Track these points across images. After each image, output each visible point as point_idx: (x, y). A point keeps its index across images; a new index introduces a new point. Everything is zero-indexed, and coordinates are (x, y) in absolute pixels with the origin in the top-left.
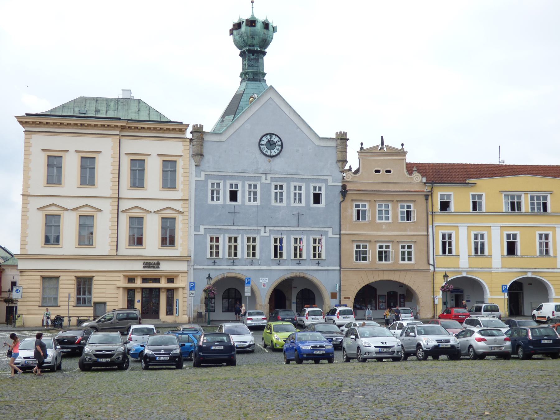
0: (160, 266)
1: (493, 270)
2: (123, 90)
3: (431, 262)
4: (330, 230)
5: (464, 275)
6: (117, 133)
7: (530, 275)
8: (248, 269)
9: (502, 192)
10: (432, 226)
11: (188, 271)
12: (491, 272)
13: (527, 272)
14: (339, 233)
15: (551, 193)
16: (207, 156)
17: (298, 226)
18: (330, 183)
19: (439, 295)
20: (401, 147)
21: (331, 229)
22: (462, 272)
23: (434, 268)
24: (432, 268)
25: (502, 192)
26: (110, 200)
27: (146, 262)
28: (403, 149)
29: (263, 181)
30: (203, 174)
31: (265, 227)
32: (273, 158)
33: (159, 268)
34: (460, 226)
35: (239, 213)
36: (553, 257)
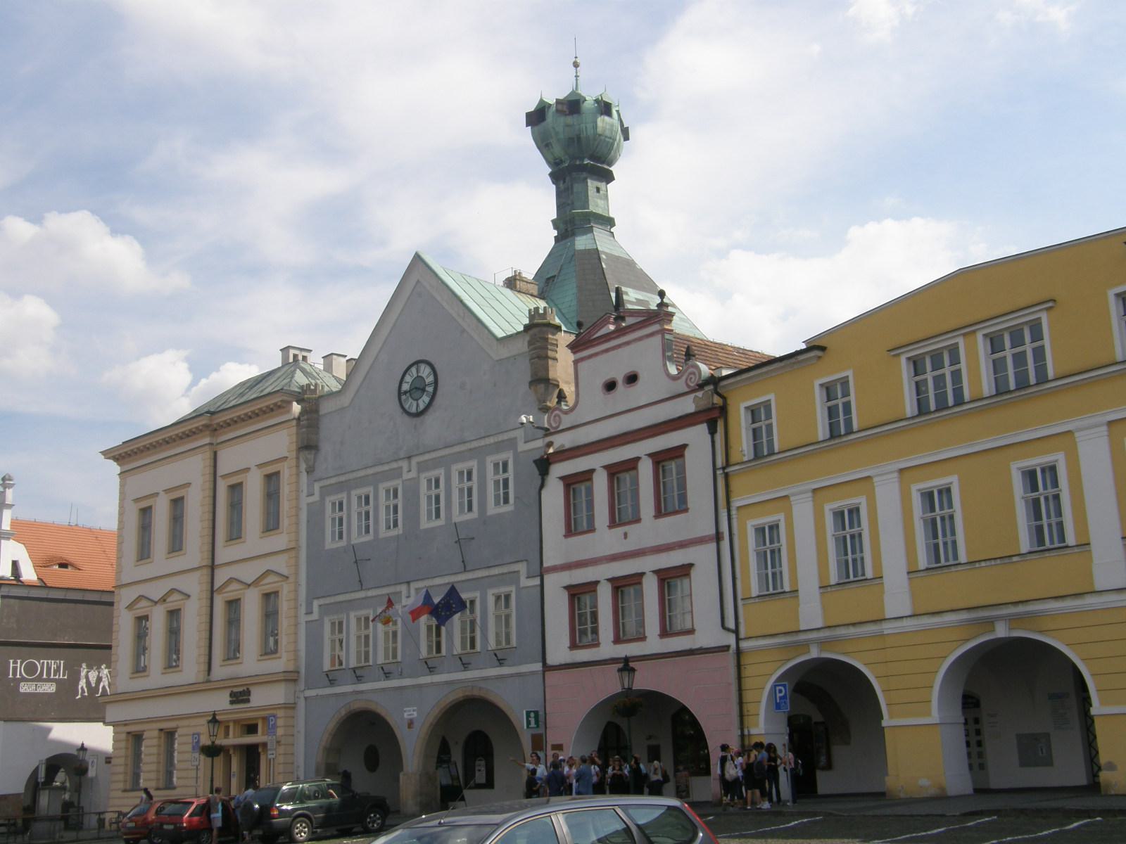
0: (252, 698)
1: (887, 628)
2: (281, 350)
3: (731, 624)
4: (522, 568)
5: (814, 653)
6: (207, 440)
7: (1001, 631)
8: (384, 690)
9: (895, 350)
10: (726, 510)
11: (295, 703)
12: (882, 635)
13: (990, 623)
14: (539, 574)
15: (1050, 303)
16: (326, 448)
17: (465, 571)
18: (522, 447)
19: (757, 725)
20: (658, 300)
21: (525, 564)
22: (805, 645)
23: (738, 639)
24: (731, 640)
25: (895, 350)
26: (197, 574)
27: (236, 690)
28: (662, 305)
29: (406, 476)
30: (317, 487)
31: (408, 583)
32: (422, 418)
33: (248, 701)
34: (794, 495)
35: (369, 560)
36: (1076, 550)
